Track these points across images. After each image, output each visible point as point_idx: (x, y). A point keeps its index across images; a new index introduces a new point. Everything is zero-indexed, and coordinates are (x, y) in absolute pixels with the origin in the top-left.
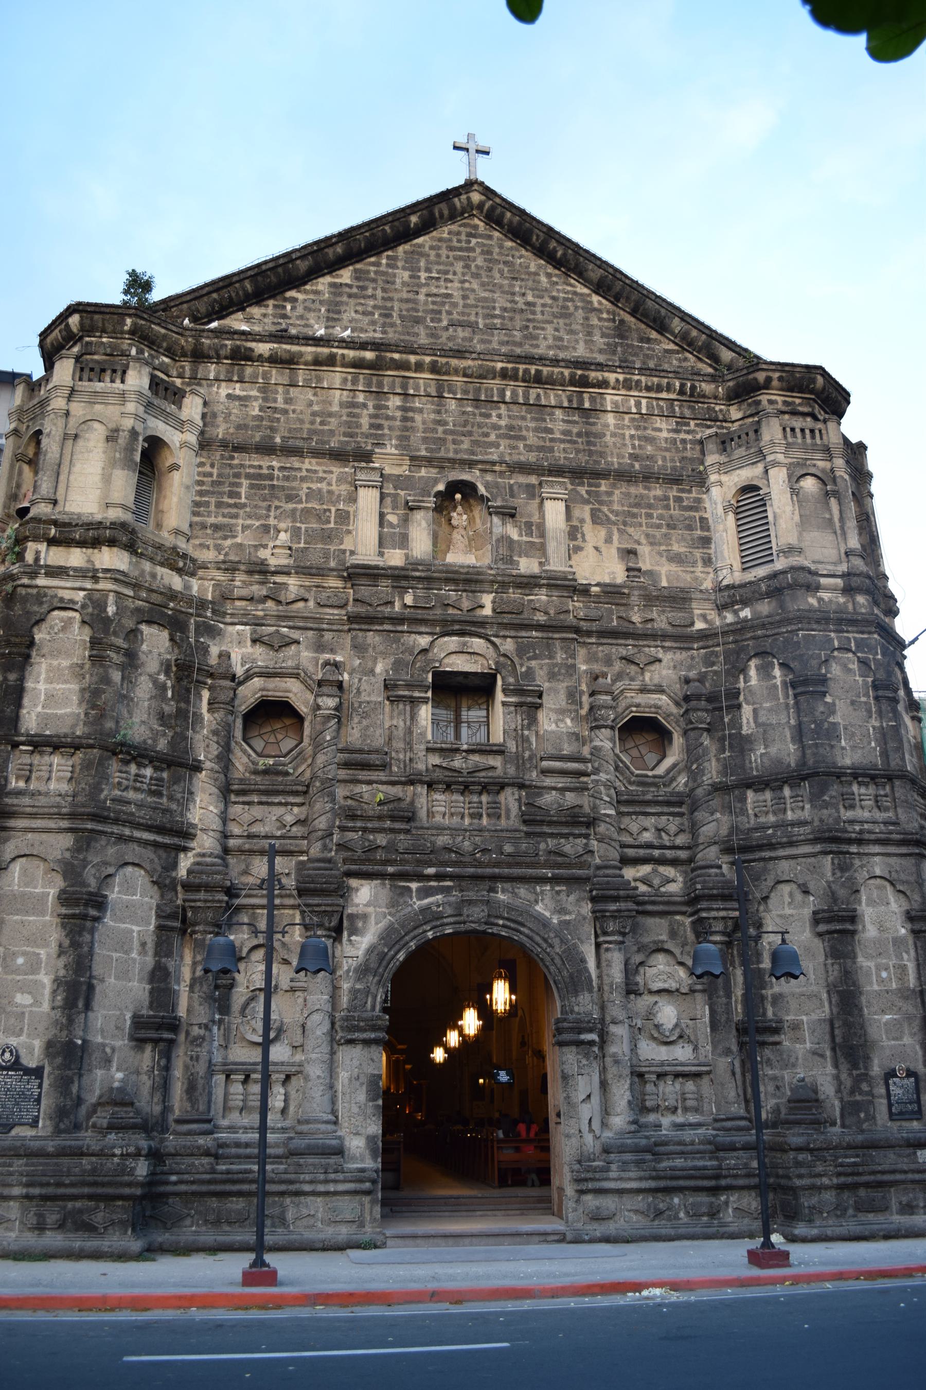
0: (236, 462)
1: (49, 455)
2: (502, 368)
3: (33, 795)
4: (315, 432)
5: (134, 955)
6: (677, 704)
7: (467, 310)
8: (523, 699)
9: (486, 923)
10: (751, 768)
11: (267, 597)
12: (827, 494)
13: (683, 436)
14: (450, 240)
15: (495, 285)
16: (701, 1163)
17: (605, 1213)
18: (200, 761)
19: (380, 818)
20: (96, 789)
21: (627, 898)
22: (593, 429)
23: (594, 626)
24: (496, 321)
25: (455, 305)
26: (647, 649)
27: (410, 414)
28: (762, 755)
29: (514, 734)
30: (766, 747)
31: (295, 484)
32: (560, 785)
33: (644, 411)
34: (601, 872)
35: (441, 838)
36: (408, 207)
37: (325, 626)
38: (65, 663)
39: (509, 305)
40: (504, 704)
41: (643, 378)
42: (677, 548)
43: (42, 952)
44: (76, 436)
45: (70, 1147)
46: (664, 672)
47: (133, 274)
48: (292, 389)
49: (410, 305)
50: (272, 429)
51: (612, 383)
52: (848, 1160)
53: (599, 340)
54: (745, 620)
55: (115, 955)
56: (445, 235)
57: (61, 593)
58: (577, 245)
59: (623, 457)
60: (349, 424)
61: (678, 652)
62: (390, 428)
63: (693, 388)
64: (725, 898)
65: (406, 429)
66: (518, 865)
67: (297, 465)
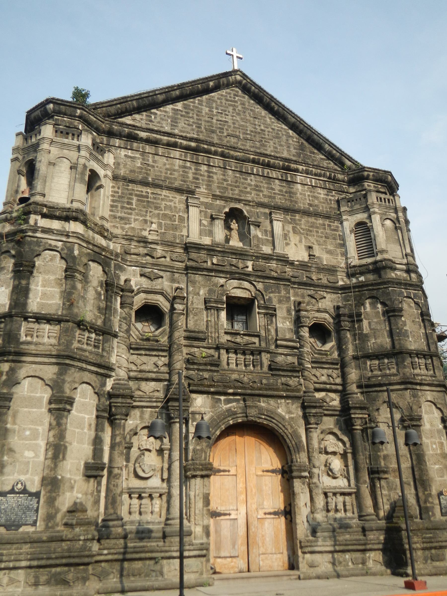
0: (130, 188)
1: (41, 172)
2: (253, 158)
3: (36, 344)
4: (168, 178)
5: (86, 430)
6: (333, 318)
7: (235, 130)
8: (267, 311)
10: (369, 349)
11: (147, 254)
12: (396, 228)
13: (330, 197)
14: (226, 96)
15: (247, 120)
16: (358, 537)
17: (316, 564)
18: (117, 332)
19: (205, 364)
20: (69, 343)
21: (321, 407)
22: (292, 190)
23: (297, 280)
24: (248, 136)
25: (229, 126)
26: (319, 292)
27: (211, 175)
28: (373, 343)
30: (375, 339)
31: (159, 201)
33: (313, 185)
34: (306, 394)
36: (209, 77)
37: (175, 271)
38: (52, 277)
39: (253, 130)
40: (259, 313)
41: (314, 170)
42: (330, 247)
43: (40, 429)
44: (54, 164)
45: (56, 536)
46: (327, 303)
47: (77, 89)
48: (156, 156)
49: (209, 124)
50: (147, 174)
52: (428, 536)
53: (293, 151)
54: (362, 281)
55: (77, 430)
56: (224, 94)
57: (50, 242)
58: (284, 106)
59: (305, 204)
60: (183, 176)
61: (333, 294)
62: (203, 180)
63: (335, 176)
64: (361, 408)
65: (210, 181)
66: (270, 389)
67: (159, 193)
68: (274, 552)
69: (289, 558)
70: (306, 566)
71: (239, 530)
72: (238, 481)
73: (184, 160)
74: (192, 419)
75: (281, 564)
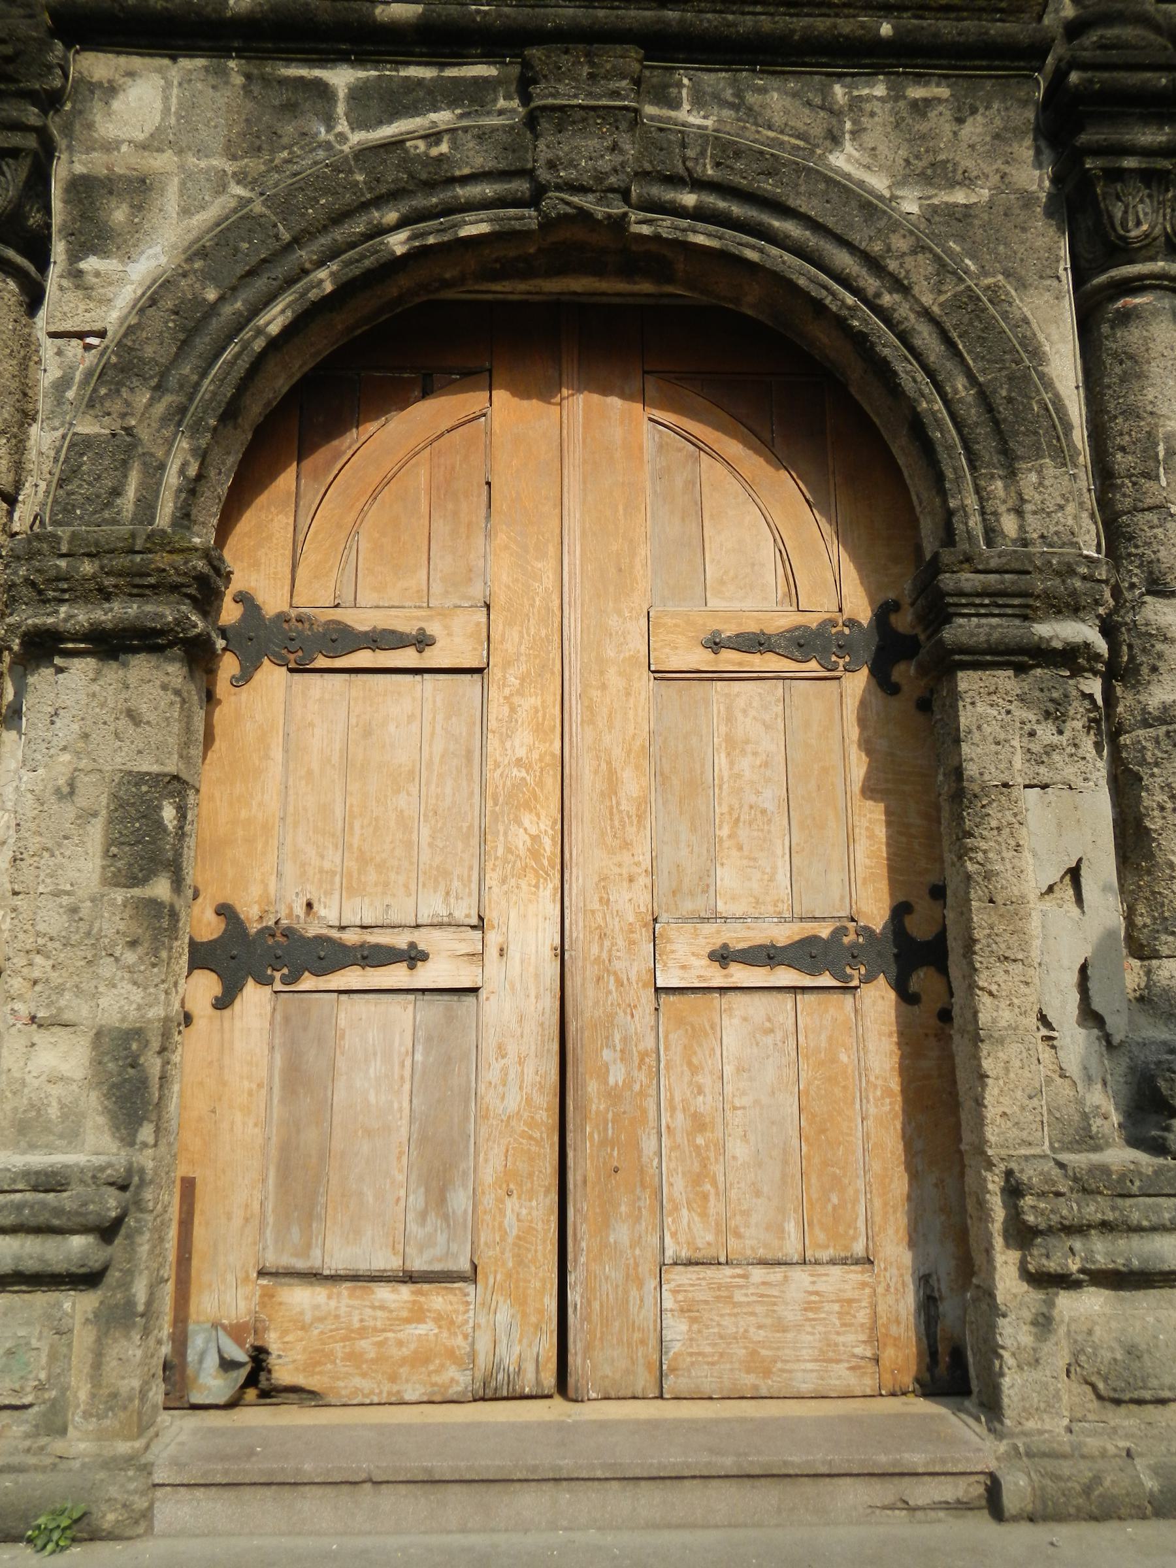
9: (625, 194)
34: (1093, 37)
68: (792, 1248)
69: (929, 1304)
70: (1072, 1394)
71: (492, 1074)
72: (497, 710)
74: (70, 234)
75: (855, 1343)
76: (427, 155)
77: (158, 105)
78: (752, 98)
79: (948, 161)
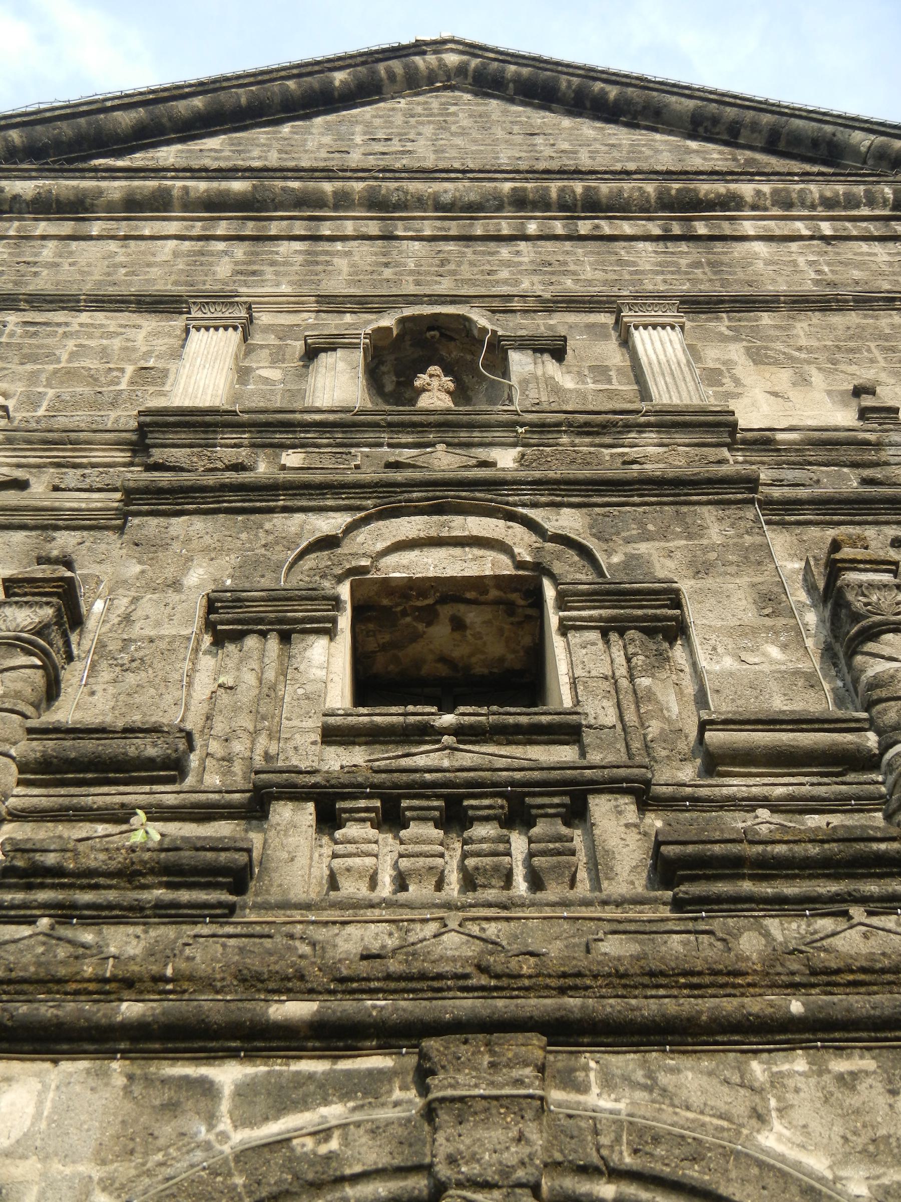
2: (514, 189)
22: (725, 259)
29: (607, 685)
32: (780, 791)
35: (350, 929)
41: (812, 187)
48: (74, 245)
51: (749, 199)
73: (199, 238)
76: (315, 1154)
77: (31, 1110)
78: (664, 1079)
79: (890, 1136)
